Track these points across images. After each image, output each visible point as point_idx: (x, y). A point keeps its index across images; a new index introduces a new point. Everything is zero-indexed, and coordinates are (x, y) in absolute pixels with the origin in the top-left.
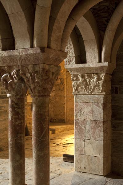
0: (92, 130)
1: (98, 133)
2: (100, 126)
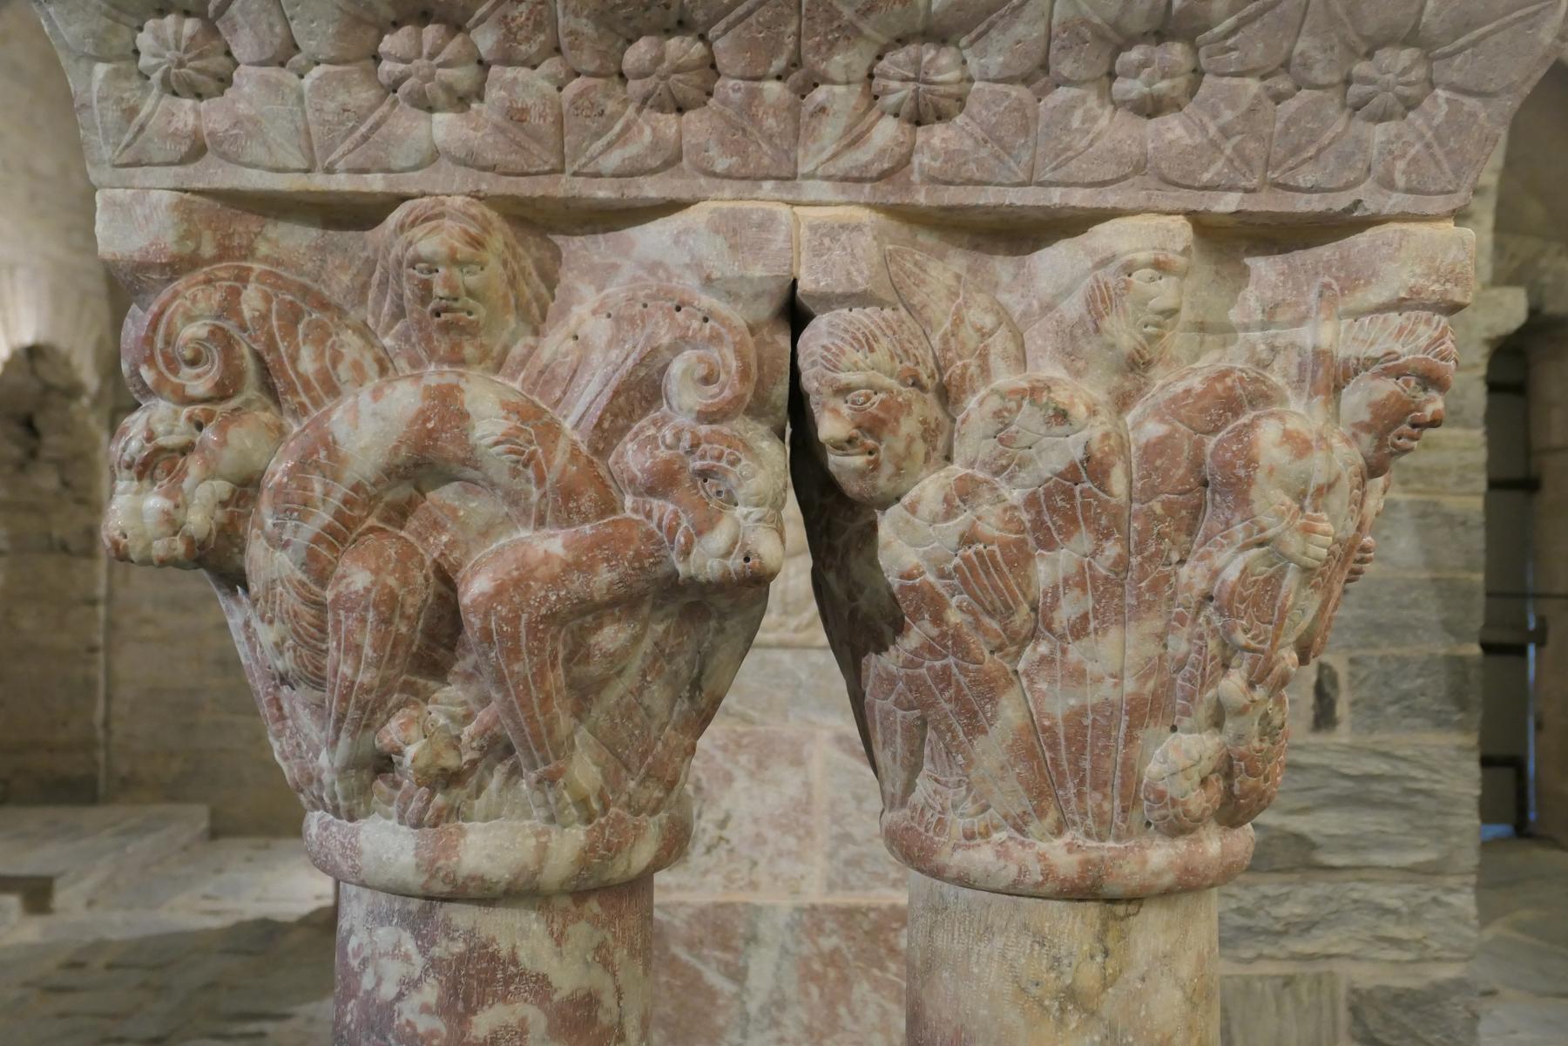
0: (814, 990)
1: (871, 1015)
2: (893, 951)
